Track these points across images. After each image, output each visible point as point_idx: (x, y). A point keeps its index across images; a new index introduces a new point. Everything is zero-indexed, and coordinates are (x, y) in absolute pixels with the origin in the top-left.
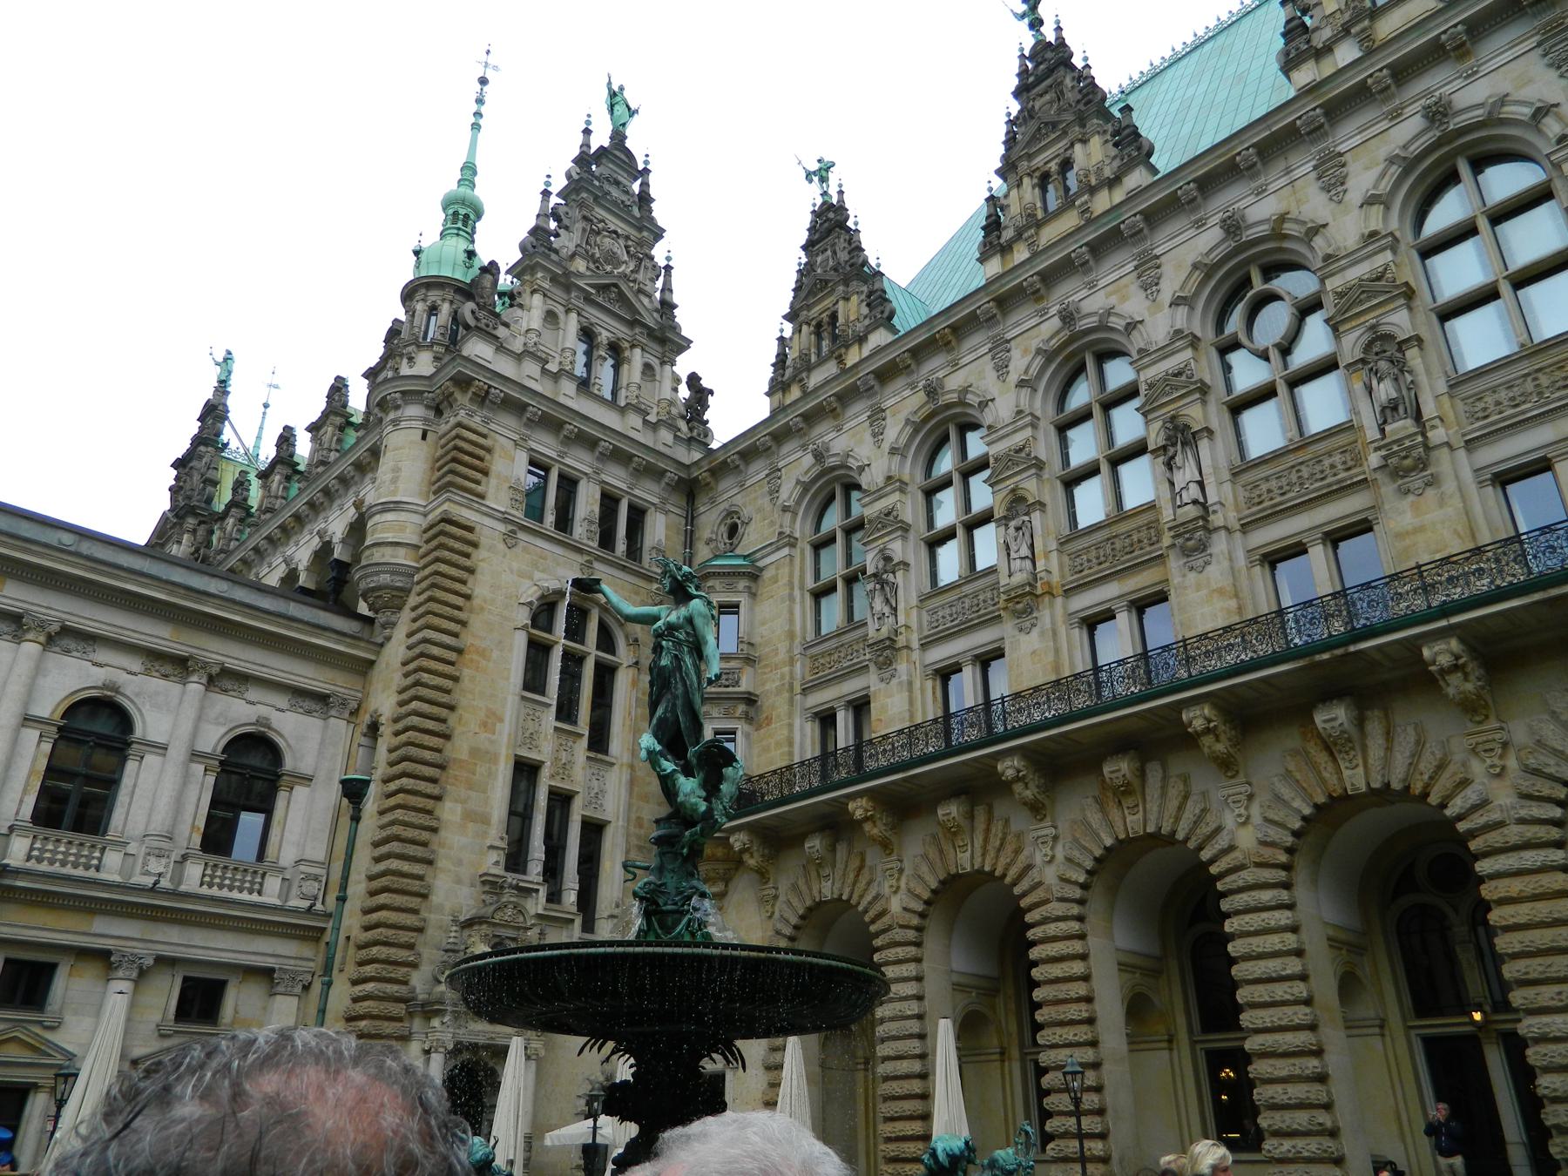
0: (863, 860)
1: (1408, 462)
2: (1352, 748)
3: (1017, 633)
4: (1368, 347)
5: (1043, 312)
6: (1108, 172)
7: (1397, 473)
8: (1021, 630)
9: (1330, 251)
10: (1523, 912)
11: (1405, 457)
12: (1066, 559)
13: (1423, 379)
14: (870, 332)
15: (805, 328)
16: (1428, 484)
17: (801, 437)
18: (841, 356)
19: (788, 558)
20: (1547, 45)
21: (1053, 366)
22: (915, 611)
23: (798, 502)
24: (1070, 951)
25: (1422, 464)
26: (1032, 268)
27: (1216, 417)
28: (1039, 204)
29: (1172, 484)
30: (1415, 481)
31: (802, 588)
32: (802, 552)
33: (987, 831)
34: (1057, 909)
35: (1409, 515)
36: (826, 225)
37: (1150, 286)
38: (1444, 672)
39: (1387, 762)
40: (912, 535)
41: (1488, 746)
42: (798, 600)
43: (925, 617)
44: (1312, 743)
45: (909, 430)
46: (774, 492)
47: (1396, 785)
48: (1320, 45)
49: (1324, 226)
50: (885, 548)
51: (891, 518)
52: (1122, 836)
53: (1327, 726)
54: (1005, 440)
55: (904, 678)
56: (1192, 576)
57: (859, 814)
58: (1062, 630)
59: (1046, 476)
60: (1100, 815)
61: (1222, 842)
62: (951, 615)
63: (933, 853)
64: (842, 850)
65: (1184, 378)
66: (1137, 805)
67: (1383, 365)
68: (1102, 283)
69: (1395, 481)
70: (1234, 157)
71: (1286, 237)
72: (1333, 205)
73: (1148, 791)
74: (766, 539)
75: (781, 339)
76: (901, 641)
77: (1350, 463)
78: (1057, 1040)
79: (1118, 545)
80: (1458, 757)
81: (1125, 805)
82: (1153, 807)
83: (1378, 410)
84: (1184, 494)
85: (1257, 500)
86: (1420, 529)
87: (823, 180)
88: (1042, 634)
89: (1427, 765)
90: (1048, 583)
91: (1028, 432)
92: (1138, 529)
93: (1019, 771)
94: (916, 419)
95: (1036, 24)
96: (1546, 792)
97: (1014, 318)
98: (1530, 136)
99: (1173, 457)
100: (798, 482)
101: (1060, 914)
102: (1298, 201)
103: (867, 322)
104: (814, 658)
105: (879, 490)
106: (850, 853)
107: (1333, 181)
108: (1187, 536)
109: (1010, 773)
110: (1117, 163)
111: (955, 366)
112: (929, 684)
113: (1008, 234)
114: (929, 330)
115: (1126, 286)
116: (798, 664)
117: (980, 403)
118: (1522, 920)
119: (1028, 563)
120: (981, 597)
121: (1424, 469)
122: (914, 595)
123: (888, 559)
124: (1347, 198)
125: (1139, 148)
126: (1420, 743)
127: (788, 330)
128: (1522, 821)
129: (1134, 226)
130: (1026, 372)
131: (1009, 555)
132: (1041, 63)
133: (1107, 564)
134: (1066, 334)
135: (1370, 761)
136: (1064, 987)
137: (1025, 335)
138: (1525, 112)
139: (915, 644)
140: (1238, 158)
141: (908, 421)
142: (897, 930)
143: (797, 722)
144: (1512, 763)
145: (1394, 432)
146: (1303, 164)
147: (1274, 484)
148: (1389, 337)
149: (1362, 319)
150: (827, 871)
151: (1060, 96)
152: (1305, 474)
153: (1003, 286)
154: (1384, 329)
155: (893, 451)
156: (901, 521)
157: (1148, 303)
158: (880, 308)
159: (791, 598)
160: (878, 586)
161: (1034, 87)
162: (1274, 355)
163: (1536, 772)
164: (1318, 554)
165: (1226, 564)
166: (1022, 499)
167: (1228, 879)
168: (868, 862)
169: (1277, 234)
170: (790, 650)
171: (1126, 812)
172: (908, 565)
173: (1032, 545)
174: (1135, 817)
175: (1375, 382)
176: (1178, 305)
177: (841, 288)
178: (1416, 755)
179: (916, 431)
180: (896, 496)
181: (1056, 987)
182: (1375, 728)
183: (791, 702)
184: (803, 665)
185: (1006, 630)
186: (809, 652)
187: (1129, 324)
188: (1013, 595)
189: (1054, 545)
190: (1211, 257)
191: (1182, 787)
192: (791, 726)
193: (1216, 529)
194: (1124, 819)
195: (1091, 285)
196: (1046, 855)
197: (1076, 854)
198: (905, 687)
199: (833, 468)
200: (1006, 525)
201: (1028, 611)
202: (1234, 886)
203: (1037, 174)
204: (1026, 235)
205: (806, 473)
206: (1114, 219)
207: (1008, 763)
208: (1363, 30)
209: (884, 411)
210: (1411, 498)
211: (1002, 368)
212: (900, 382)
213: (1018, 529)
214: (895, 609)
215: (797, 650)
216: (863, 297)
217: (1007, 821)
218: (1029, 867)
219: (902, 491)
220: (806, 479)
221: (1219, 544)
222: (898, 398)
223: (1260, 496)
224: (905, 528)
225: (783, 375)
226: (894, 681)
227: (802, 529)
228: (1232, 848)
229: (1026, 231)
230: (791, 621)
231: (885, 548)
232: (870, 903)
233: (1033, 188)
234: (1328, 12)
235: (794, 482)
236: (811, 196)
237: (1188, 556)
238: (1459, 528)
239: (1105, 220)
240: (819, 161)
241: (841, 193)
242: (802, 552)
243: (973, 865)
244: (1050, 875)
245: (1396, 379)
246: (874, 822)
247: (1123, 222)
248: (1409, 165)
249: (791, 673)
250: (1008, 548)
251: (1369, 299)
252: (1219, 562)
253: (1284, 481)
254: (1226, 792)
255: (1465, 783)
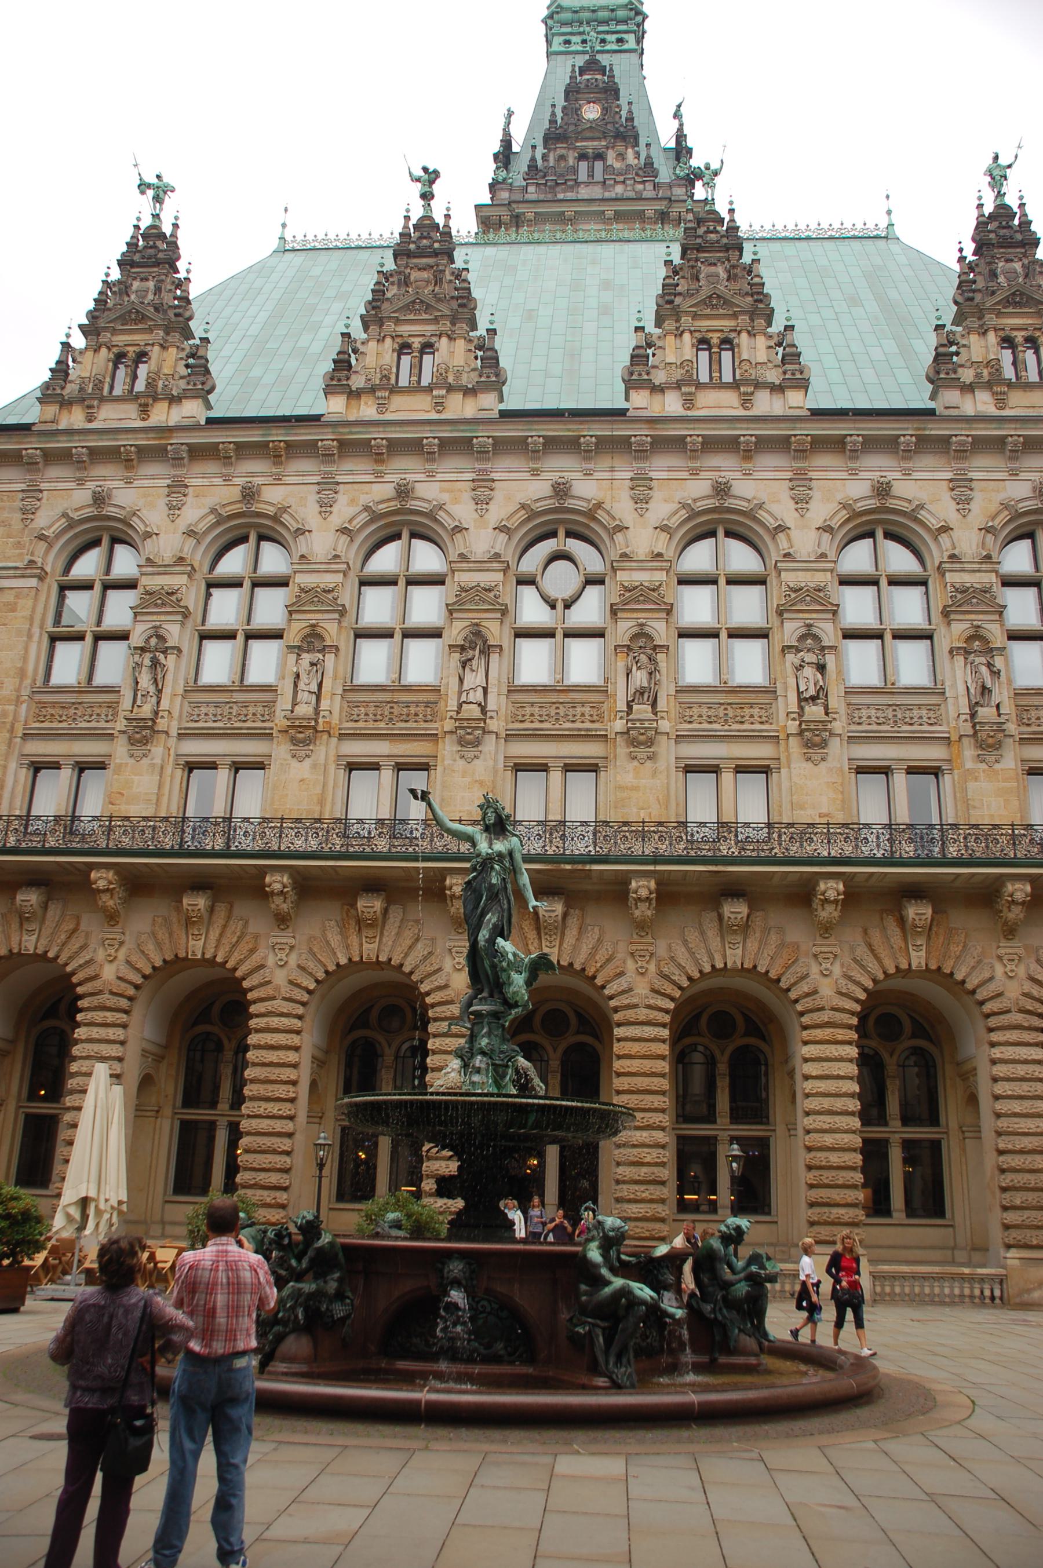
0: (78, 924)
1: (642, 738)
2: (555, 934)
3: (289, 757)
4: (635, 637)
5: (379, 474)
6: (469, 379)
7: (633, 742)
8: (294, 756)
9: (627, 551)
10: (634, 1065)
11: (643, 734)
12: (346, 705)
13: (664, 678)
14: (186, 398)
15: (104, 351)
16: (649, 758)
17: (79, 469)
18: (147, 405)
19: (34, 591)
20: (795, 483)
21: (374, 527)
22: (179, 698)
23: (58, 536)
24: (289, 1043)
25: (650, 742)
26: (384, 432)
27: (506, 641)
28: (394, 370)
29: (461, 680)
30: (642, 752)
31: (41, 627)
32: (49, 587)
33: (225, 927)
34: (286, 1007)
35: (631, 775)
36: (152, 251)
37: (482, 502)
38: (639, 899)
39: (575, 948)
40: (190, 624)
41: (643, 954)
42: (36, 638)
43: (187, 708)
44: (527, 922)
45: (212, 519)
46: (28, 513)
47: (577, 966)
48: (657, 383)
49: (627, 528)
50: (160, 627)
51: (174, 598)
52: (356, 959)
53: (546, 914)
54: (314, 575)
55: (158, 761)
56: (461, 763)
57: (101, 884)
58: (332, 767)
59: (344, 624)
60: (339, 937)
61: (439, 980)
62: (215, 715)
63: (162, 935)
64: (54, 911)
65: (491, 595)
66: (375, 937)
67: (643, 658)
68: (439, 477)
69: (628, 747)
70: (580, 437)
71: (595, 519)
72: (636, 515)
73: (387, 927)
74: (7, 559)
75: (66, 346)
76: (162, 724)
77: (595, 718)
78: (261, 1111)
79: (396, 711)
80: (619, 956)
81: (364, 934)
82: (388, 940)
83: (632, 691)
84: (471, 692)
85: (520, 718)
86: (635, 789)
87: (158, 199)
88: (314, 766)
89: (601, 957)
90: (329, 723)
91: (339, 578)
92: (417, 704)
93: (284, 887)
94: (224, 512)
95: (427, 197)
96: (668, 991)
97: (348, 465)
98: (767, 538)
99: (470, 660)
100: (65, 515)
101: (285, 1011)
102: (613, 497)
103: (182, 384)
104: (42, 705)
105: (165, 566)
106: (63, 915)
107: (642, 497)
108: (469, 730)
109: (277, 887)
110: (474, 377)
111: (278, 480)
112: (179, 773)
113: (357, 382)
114: (263, 435)
115: (460, 490)
116: (24, 706)
117: (298, 529)
118: (633, 1070)
119: (314, 697)
120: (251, 710)
121: (649, 747)
122: (181, 683)
123: (161, 638)
124: (647, 515)
125: (497, 375)
126: (600, 941)
127: (79, 341)
128: (649, 1007)
129: (484, 446)
130: (350, 521)
131: (296, 685)
132: (425, 238)
133: (382, 725)
134: (395, 505)
135: (565, 945)
136: (277, 1070)
137: (355, 486)
138: (772, 523)
139: (174, 732)
140: (582, 440)
141: (213, 511)
142: (107, 996)
143: (13, 765)
144: (652, 967)
145: (639, 712)
146: (624, 471)
147: (536, 710)
148: (649, 637)
149: (635, 615)
150: (34, 926)
151: (438, 281)
152: (562, 712)
153: (351, 433)
154: (647, 629)
155: (190, 533)
156: (186, 607)
157: (476, 516)
158: (202, 379)
159: (30, 636)
160: (147, 662)
161: (415, 257)
162: (560, 606)
163: (666, 977)
164: (556, 776)
165: (491, 763)
166: (321, 638)
167: (438, 1009)
168: (83, 927)
169: (591, 515)
170: (18, 690)
171: (364, 940)
172: (180, 651)
173: (321, 682)
174: (372, 946)
175: (634, 668)
176: (501, 531)
177: (161, 333)
178: (595, 950)
179: (218, 523)
180: (184, 579)
181: (268, 1069)
182: (573, 923)
183: (10, 743)
184: (28, 710)
185: (280, 751)
186: (37, 697)
187: (457, 526)
188: (297, 724)
189: (340, 691)
190: (538, 505)
191: (416, 931)
192: (5, 767)
193: (490, 732)
194: (361, 945)
195: (431, 474)
196: (281, 960)
197: (311, 965)
198: (157, 770)
199: (109, 518)
200: (299, 655)
201: (307, 742)
202: (443, 1015)
203: (399, 340)
204: (379, 394)
205: (77, 510)
206: (470, 431)
207: (277, 877)
208: (690, 394)
209: (186, 486)
210: (636, 763)
211: (326, 507)
212: (212, 467)
213: (312, 664)
214: (160, 691)
215: (25, 692)
216: (183, 355)
217: (247, 922)
218: (262, 966)
219: (190, 576)
220: (75, 516)
221: (489, 745)
222: (206, 482)
223: (524, 716)
224: (186, 614)
225: (63, 388)
226: (145, 761)
227: (52, 562)
228: (446, 986)
229: (380, 390)
230: (25, 659)
231: (160, 627)
232: (80, 966)
233: (393, 351)
234: (668, 360)
235: (59, 510)
236: (143, 208)
237: (462, 746)
238: (661, 797)
239: (462, 428)
240: (158, 177)
241: (176, 226)
242: (49, 587)
243: (203, 954)
244: (280, 978)
245: (650, 674)
246: (112, 895)
247: (477, 437)
248: (693, 515)
249: (16, 713)
250: (298, 676)
251: (644, 602)
252: (485, 760)
253: (544, 712)
254: (452, 944)
255: (621, 974)
